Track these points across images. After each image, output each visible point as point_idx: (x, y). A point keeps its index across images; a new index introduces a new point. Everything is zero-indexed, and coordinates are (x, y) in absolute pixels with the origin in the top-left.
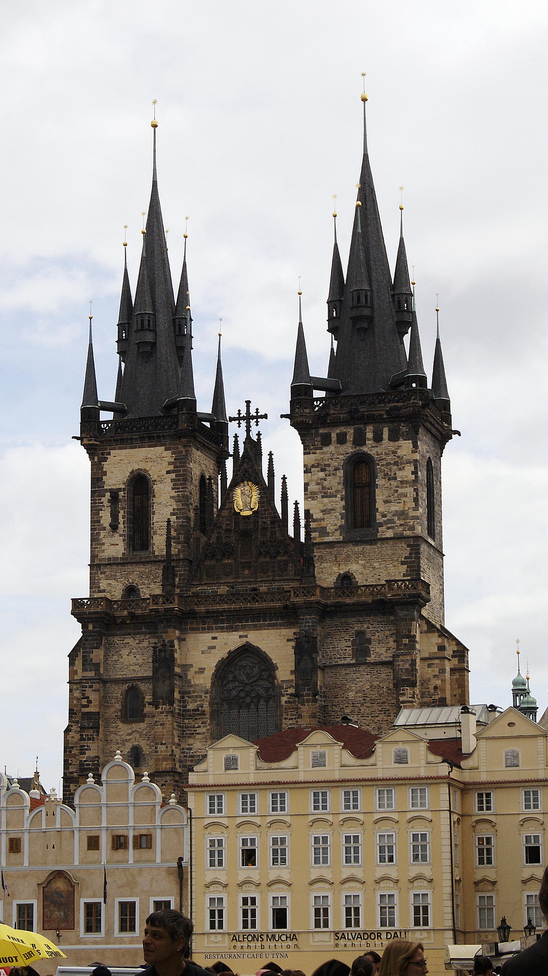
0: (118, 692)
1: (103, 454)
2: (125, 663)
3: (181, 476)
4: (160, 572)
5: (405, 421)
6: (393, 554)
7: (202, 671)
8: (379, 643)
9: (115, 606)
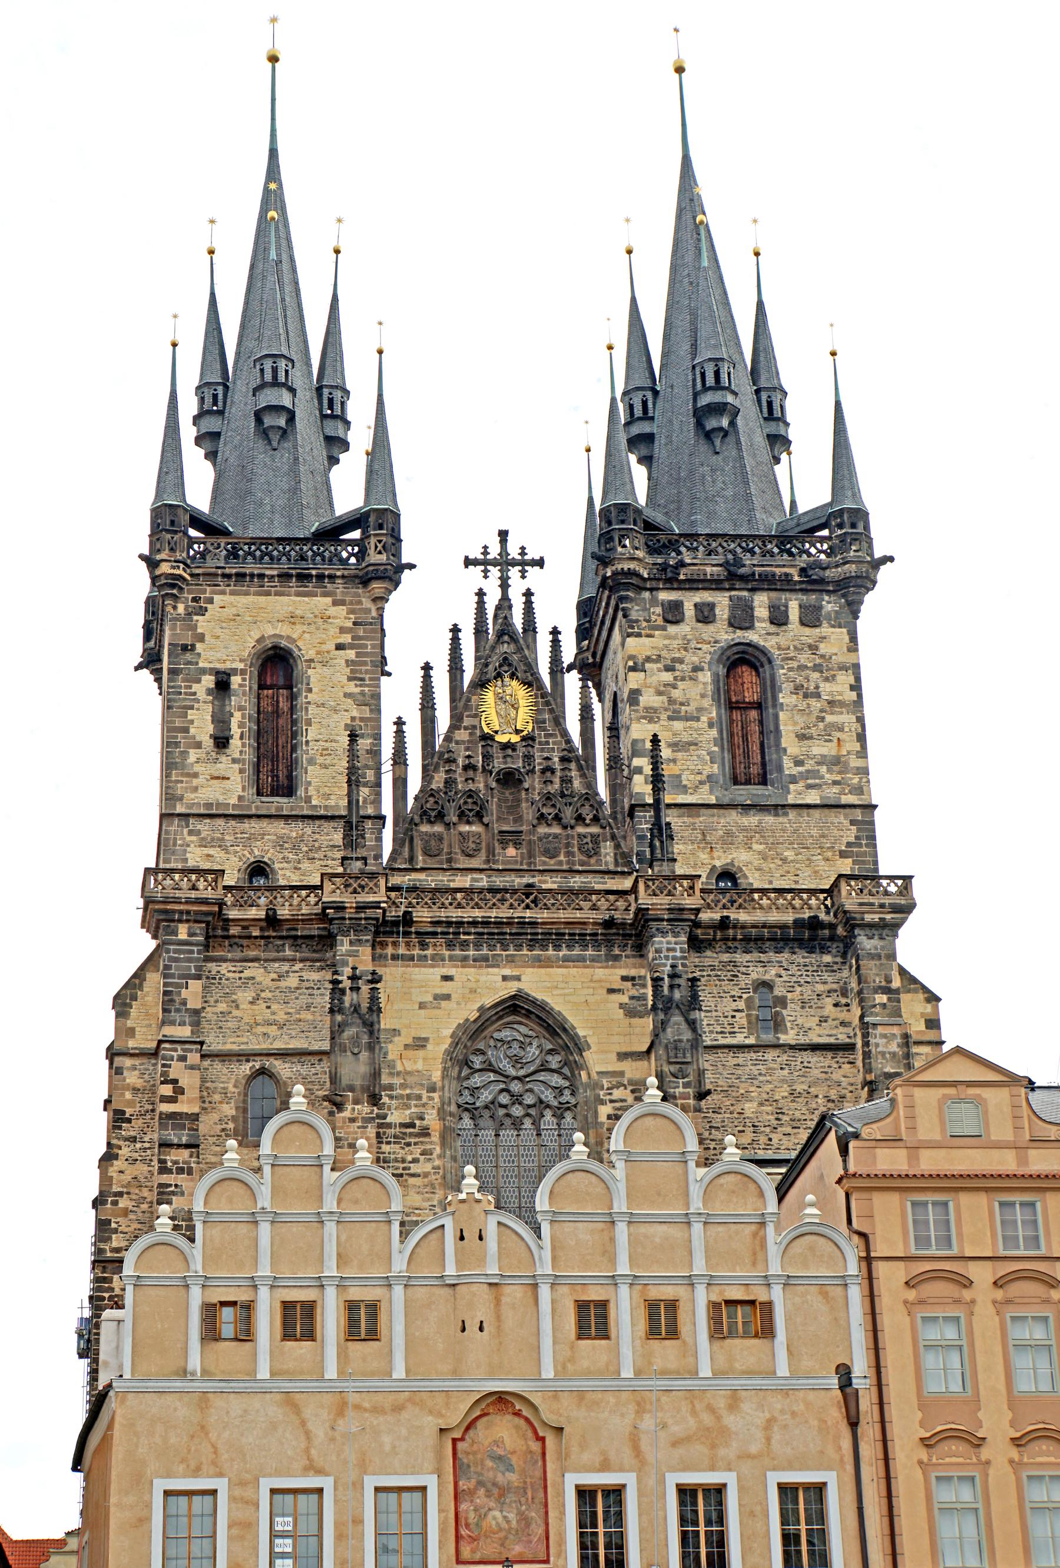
2: (246, 1019)
5: (834, 591)
6: (821, 836)
7: (420, 1043)
8: (803, 1007)
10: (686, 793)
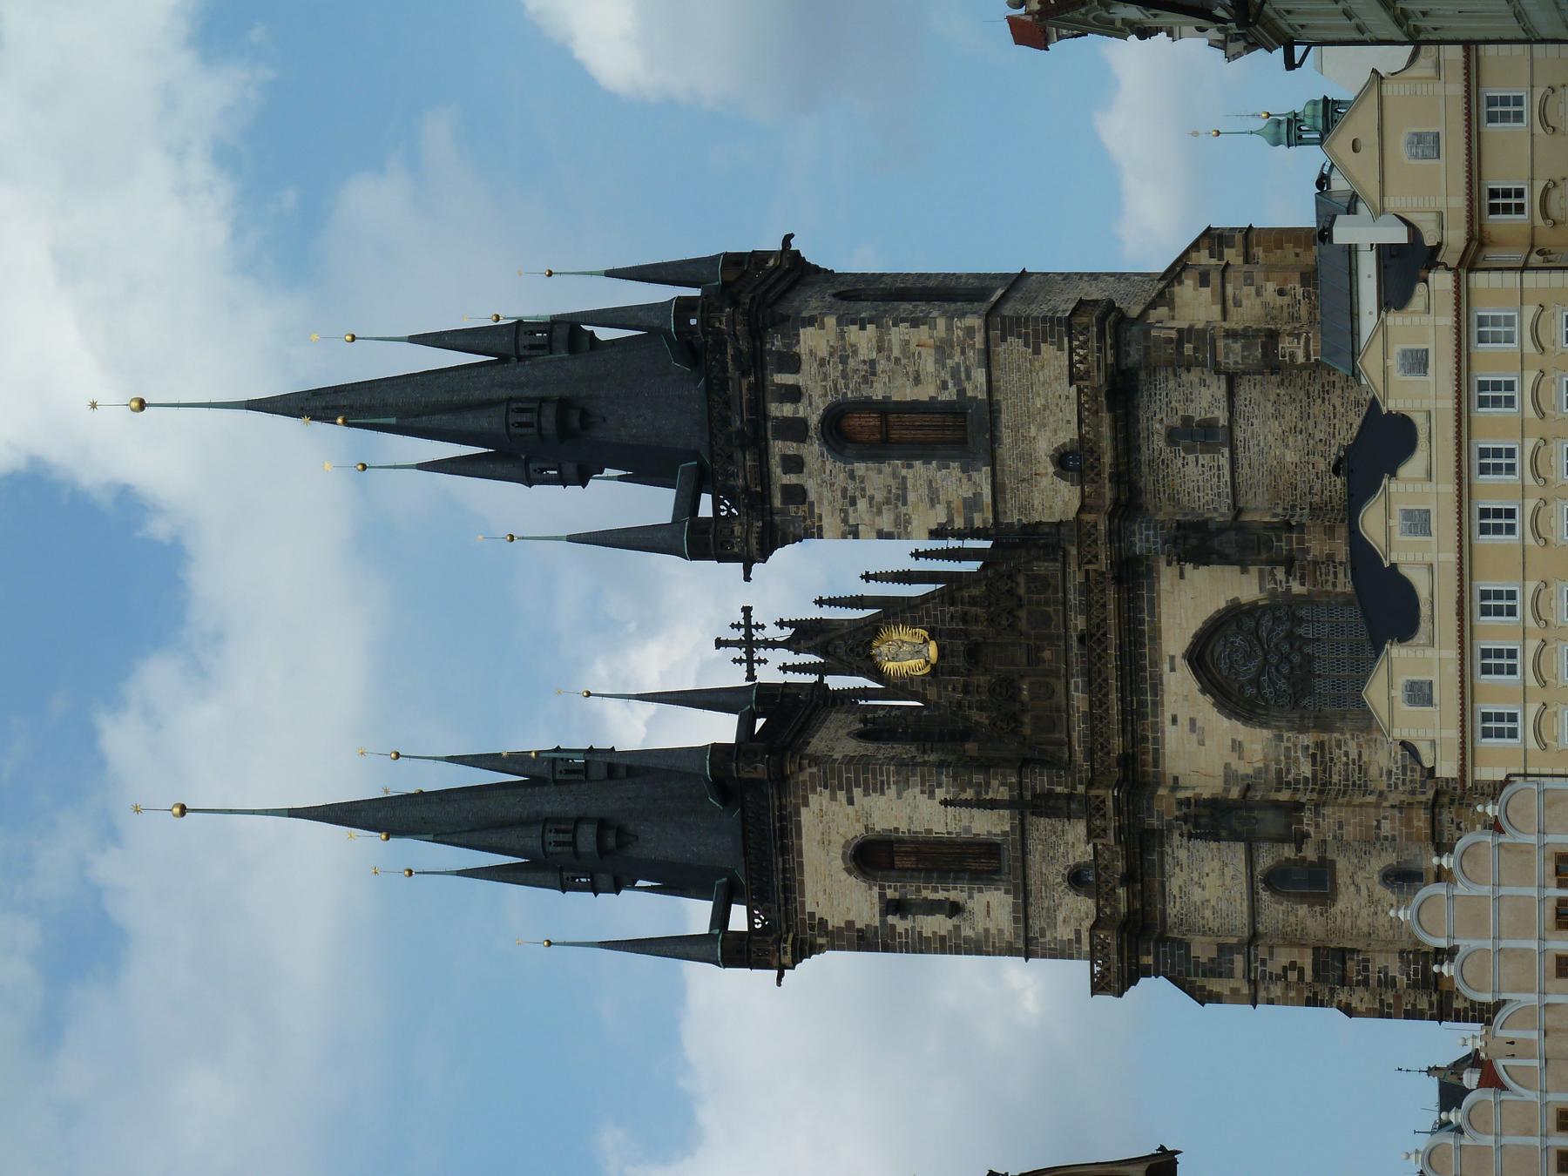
0: (1275, 911)
1: (812, 928)
3: (855, 776)
4: (1043, 821)
6: (1019, 369)
7: (1237, 746)
9: (1108, 911)
10: (981, 494)
